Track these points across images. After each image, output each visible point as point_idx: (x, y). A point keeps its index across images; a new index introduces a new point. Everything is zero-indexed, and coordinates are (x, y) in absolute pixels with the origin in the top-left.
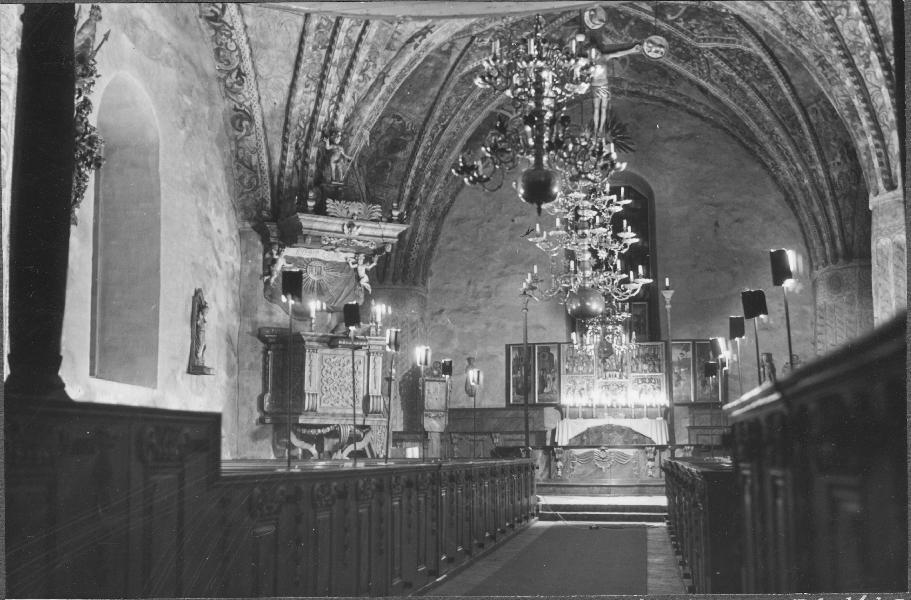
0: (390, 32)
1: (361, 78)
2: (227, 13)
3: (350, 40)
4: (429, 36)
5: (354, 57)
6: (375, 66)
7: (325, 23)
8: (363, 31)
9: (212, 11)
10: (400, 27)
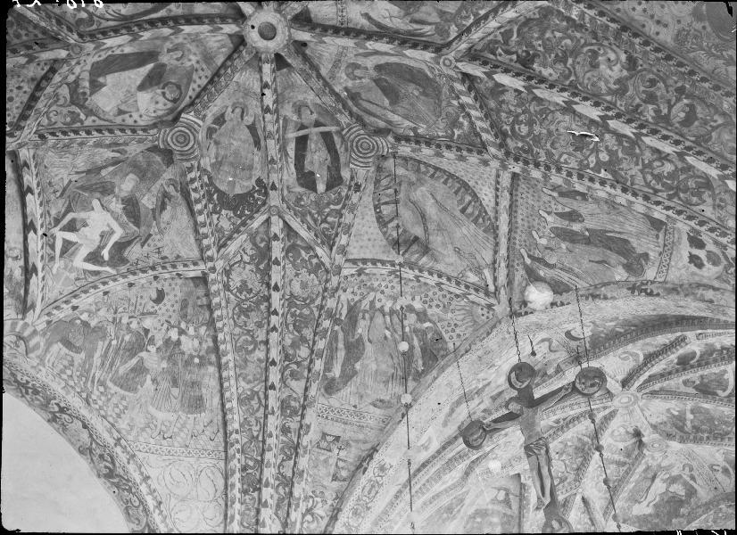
0: (332, 461)
1: (309, 517)
2: (117, 465)
3: (284, 477)
4: (376, 456)
5: (291, 493)
6: (324, 502)
7: (251, 463)
8: (295, 463)
9: (106, 467)
10: (343, 454)
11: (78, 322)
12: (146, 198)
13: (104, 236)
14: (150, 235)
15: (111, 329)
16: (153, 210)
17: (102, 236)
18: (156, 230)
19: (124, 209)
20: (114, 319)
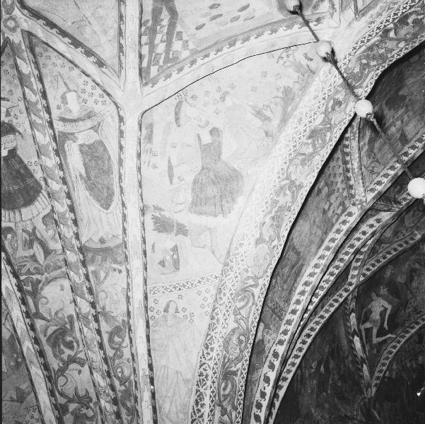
11: (386, 380)
12: (399, 277)
13: (382, 314)
14: (408, 301)
15: (405, 375)
16: (406, 283)
17: (381, 315)
18: (411, 296)
19: (388, 290)
20: (403, 367)
